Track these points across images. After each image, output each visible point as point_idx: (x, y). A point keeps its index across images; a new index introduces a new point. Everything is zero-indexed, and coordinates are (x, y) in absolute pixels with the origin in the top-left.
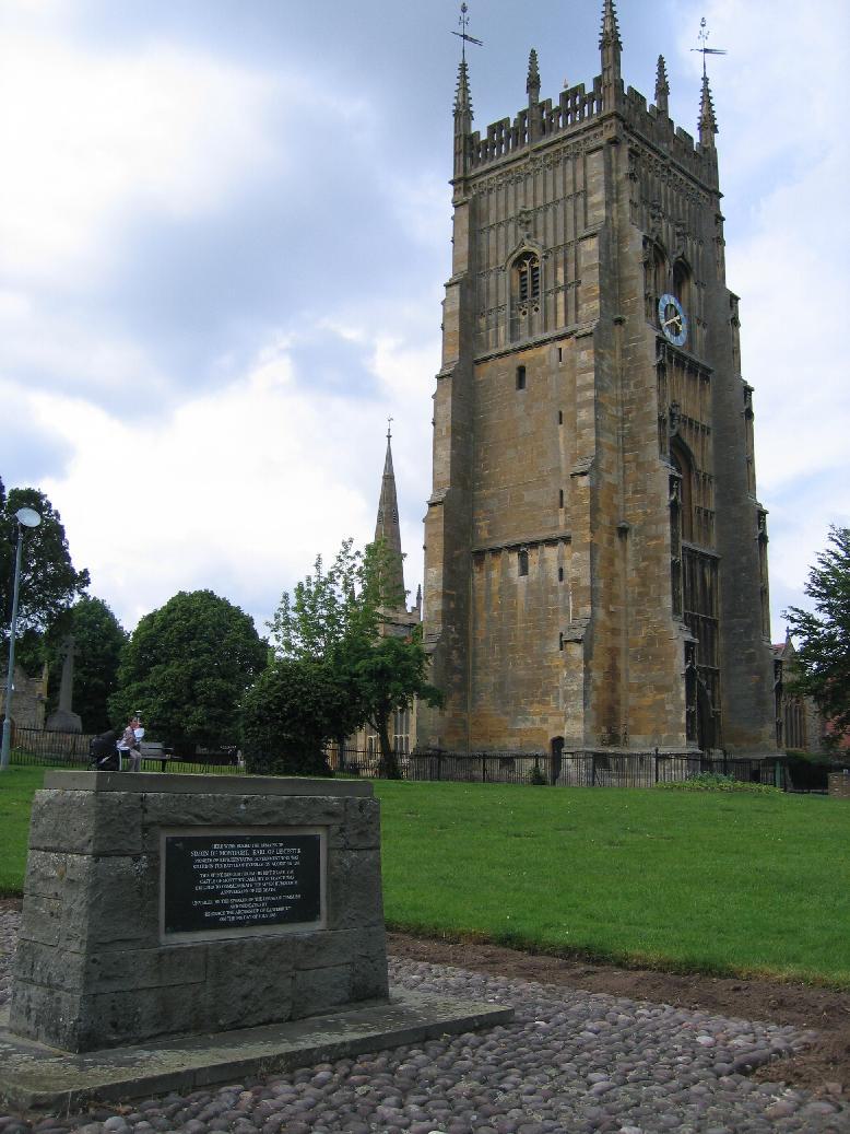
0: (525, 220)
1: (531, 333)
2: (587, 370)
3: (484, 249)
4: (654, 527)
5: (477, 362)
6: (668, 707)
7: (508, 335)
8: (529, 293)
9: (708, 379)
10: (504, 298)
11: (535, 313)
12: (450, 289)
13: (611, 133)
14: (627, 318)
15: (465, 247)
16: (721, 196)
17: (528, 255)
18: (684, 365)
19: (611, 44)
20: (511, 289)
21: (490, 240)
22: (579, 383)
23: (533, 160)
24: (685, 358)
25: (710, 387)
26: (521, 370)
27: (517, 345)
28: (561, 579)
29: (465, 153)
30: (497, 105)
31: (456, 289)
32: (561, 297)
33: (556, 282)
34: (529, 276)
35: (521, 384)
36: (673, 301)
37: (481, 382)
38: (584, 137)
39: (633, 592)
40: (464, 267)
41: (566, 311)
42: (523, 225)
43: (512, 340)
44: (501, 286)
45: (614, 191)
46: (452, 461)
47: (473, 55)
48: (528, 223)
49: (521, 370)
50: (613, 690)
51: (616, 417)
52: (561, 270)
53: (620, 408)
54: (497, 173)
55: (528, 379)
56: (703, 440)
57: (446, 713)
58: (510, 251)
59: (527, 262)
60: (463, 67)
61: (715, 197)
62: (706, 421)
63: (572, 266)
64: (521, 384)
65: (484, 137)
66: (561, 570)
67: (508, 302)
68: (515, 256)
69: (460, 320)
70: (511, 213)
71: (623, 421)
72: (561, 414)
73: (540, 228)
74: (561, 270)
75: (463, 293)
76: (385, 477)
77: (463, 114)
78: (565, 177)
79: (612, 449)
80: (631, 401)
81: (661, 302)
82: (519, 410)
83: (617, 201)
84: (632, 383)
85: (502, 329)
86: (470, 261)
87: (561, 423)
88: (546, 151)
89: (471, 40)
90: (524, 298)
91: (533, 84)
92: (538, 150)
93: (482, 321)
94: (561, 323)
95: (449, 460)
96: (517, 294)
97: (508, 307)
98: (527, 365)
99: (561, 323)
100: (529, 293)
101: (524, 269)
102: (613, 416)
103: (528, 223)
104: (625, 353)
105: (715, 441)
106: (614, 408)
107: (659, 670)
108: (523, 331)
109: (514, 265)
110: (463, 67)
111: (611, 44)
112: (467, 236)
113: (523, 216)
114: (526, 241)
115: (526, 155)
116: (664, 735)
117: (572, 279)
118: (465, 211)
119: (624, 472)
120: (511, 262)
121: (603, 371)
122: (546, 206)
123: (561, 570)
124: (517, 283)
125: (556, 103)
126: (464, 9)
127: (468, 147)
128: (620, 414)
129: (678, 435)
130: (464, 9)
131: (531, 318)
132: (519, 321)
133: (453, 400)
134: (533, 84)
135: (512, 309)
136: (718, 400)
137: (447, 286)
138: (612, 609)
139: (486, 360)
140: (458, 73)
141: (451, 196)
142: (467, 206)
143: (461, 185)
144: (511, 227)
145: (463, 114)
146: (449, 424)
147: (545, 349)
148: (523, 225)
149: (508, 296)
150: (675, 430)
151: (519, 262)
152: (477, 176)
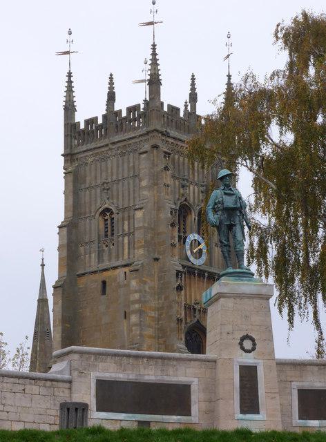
0: (106, 187)
1: (110, 260)
2: (136, 292)
3: (83, 202)
5: (79, 276)
7: (97, 260)
8: (109, 233)
10: (94, 237)
11: (112, 247)
12: (62, 229)
13: (153, 142)
14: (161, 257)
15: (71, 202)
17: (108, 210)
18: (204, 276)
19: (154, 82)
20: (99, 230)
22: (132, 299)
24: (205, 271)
26: (104, 283)
27: (102, 266)
29: (71, 136)
30: (90, 108)
31: (65, 229)
32: (126, 240)
33: (123, 230)
34: (109, 222)
35: (104, 291)
36: (196, 236)
37: (81, 288)
38: (139, 140)
40: (70, 214)
41: (129, 248)
42: (106, 191)
43: (99, 262)
44: (94, 226)
46: (62, 341)
48: (108, 189)
49: (104, 283)
52: (126, 223)
53: (157, 312)
55: (107, 288)
59: (108, 214)
60: (70, 75)
64: (104, 291)
68: (100, 210)
69: (68, 250)
70: (99, 182)
71: (159, 320)
72: (125, 312)
73: (115, 194)
74: (126, 223)
75: (69, 233)
76: (39, 301)
77: (70, 108)
78: (129, 164)
79: (150, 337)
80: (162, 308)
81: (187, 240)
82: (102, 308)
83: (157, 184)
84: (163, 297)
85: (93, 255)
86: (74, 211)
87: (125, 318)
88: (119, 145)
90: (106, 236)
91: (111, 97)
92: (113, 143)
93: (82, 249)
94: (126, 257)
95: (60, 339)
96: (102, 233)
97: (96, 242)
98: (107, 280)
99: (126, 257)
100: (109, 233)
101: (106, 218)
102: (153, 317)
103: (108, 189)
104: (160, 278)
108: (106, 257)
110: (70, 75)
111: (154, 82)
112: (71, 194)
114: (107, 201)
115: (107, 145)
118: (71, 178)
120: (98, 213)
121: (145, 291)
124: (102, 226)
125: (124, 114)
127: (71, 129)
128: (157, 316)
129: (198, 321)
131: (110, 250)
132: (103, 250)
133: (63, 302)
134: (111, 97)
135: (99, 243)
137: (60, 227)
139: (83, 274)
140: (67, 79)
141: (62, 164)
144: (99, 190)
145: (70, 108)
146: (60, 317)
147: (117, 271)
148: (106, 191)
150: (196, 319)
151: (103, 213)
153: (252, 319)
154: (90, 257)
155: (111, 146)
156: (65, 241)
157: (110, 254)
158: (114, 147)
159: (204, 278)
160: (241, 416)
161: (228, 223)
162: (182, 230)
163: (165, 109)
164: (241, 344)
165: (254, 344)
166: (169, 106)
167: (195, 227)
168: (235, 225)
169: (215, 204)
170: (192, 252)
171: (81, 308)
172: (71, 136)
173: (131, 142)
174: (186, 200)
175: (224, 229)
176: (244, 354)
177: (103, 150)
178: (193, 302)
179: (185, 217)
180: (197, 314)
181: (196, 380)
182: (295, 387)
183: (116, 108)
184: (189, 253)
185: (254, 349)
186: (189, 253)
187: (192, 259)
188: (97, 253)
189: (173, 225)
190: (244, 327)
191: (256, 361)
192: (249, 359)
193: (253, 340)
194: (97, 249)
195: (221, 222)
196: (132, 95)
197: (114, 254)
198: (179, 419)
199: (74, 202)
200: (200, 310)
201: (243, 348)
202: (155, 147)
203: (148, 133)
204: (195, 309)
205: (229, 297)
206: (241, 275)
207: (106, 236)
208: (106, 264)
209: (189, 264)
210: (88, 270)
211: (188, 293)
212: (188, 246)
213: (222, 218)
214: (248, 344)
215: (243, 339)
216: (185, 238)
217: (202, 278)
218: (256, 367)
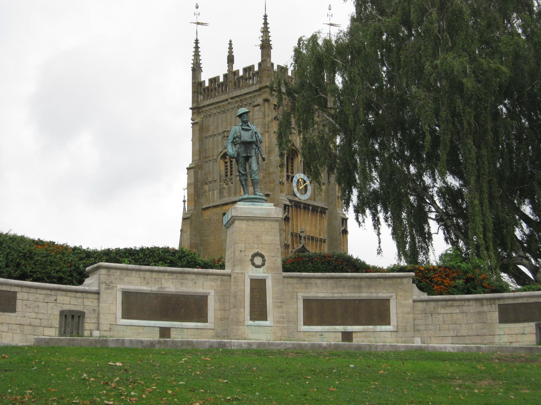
7: (219, 196)
8: (229, 174)
9: (325, 213)
10: (217, 177)
11: (231, 185)
12: (190, 170)
18: (309, 209)
19: (266, 46)
20: (220, 172)
23: (229, 103)
24: (309, 205)
25: (326, 217)
30: (214, 69)
31: (192, 170)
34: (229, 164)
36: (302, 176)
38: (254, 95)
40: (197, 158)
42: (226, 138)
45: (266, 127)
47: (203, 34)
54: (214, 106)
56: (320, 246)
60: (197, 42)
62: (324, 236)
65: (207, 84)
67: (218, 178)
68: (222, 154)
69: (195, 188)
75: (196, 174)
77: (196, 69)
81: (294, 179)
83: (268, 132)
85: (216, 192)
86: (200, 155)
89: (202, 24)
90: (227, 176)
91: (231, 60)
92: (232, 98)
93: (206, 187)
96: (223, 173)
97: (218, 181)
100: (229, 174)
101: (226, 161)
105: (329, 245)
108: (225, 194)
109: (221, 158)
110: (197, 42)
111: (266, 46)
113: (225, 133)
115: (227, 100)
118: (197, 127)
120: (220, 157)
125: (241, 73)
126: (197, 7)
127: (198, 87)
129: (303, 246)
130: (197, 7)
131: (229, 188)
132: (224, 188)
134: (231, 60)
135: (220, 182)
136: (330, 224)
137: (188, 169)
140: (194, 45)
141: (191, 116)
143: (196, 111)
145: (196, 69)
148: (226, 138)
149: (218, 175)
150: (301, 245)
152: (205, 106)
153: (263, 238)
154: (213, 194)
155: (230, 100)
156: (193, 181)
157: (229, 191)
158: (232, 101)
159: (309, 211)
160: (251, 323)
161: (245, 155)
162: (290, 170)
163: (275, 68)
164: (252, 260)
165: (264, 261)
166: (278, 66)
167: (301, 168)
168: (251, 157)
169: (234, 138)
170: (298, 189)
171: (206, 236)
172: (198, 92)
174: (293, 145)
175: (241, 160)
176: (255, 269)
177: (224, 103)
178: (299, 230)
179: (292, 159)
180: (303, 241)
181: (212, 292)
182: (301, 297)
183: (235, 69)
184: (295, 190)
185: (263, 264)
186: (295, 190)
187: (298, 194)
188: (218, 190)
189: (281, 166)
190: (256, 245)
191: (265, 275)
192: (259, 273)
193: (262, 256)
194: (219, 187)
195: (238, 155)
196: (248, 57)
197: (233, 191)
198: (196, 326)
199: (200, 147)
200: (305, 238)
201: (253, 264)
202: (266, 100)
203: (260, 89)
204: (300, 237)
205: (243, 220)
206: (254, 200)
207: (227, 176)
208: (227, 200)
209: (297, 199)
210: (212, 204)
211: (294, 223)
212: (294, 184)
213: (240, 150)
214: (258, 261)
215: (254, 256)
216: (293, 177)
217: (307, 211)
218: (265, 280)
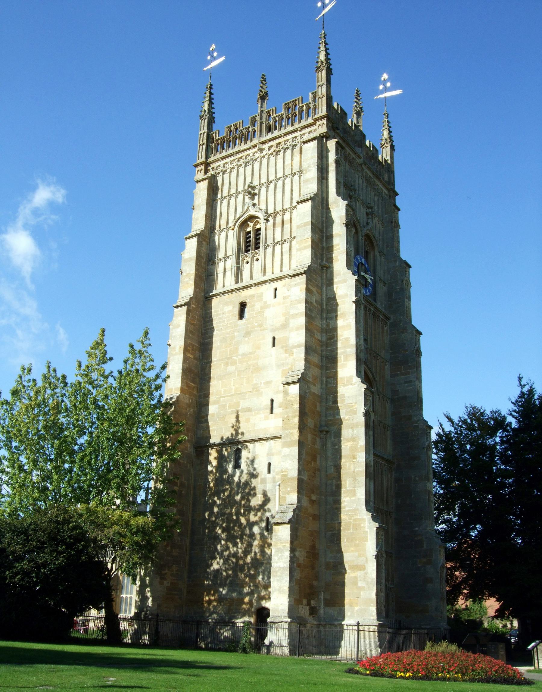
4: (350, 430)
6: (360, 584)
10: (232, 251)
16: (397, 194)
21: (222, 207)
27: (240, 285)
28: (269, 472)
35: (241, 315)
39: (332, 485)
49: (243, 306)
50: (313, 568)
51: (321, 341)
52: (278, 230)
53: (324, 334)
57: (165, 582)
58: (238, 217)
61: (392, 194)
63: (287, 226)
64: (241, 315)
66: (270, 464)
68: (242, 219)
79: (317, 366)
92: (263, 143)
98: (248, 301)
102: (319, 340)
106: (319, 334)
107: (352, 551)
115: (255, 146)
116: (357, 608)
117: (287, 236)
119: (326, 386)
122: (269, 183)
123: (270, 464)
128: (324, 339)
138: (314, 497)
142: (207, 181)
151: (244, 224)
173: (289, 137)
